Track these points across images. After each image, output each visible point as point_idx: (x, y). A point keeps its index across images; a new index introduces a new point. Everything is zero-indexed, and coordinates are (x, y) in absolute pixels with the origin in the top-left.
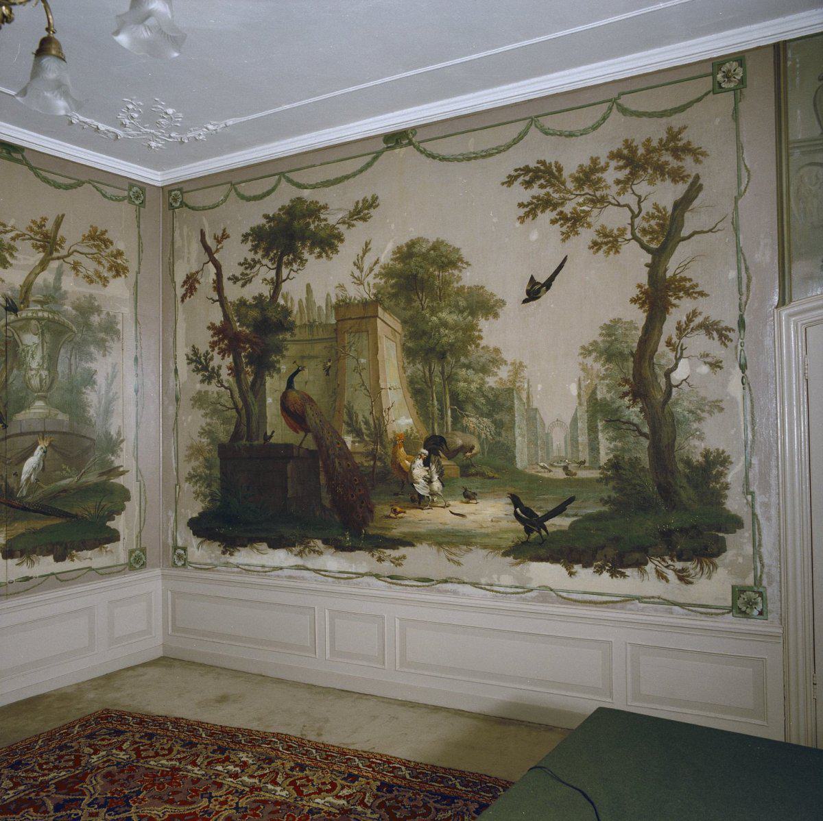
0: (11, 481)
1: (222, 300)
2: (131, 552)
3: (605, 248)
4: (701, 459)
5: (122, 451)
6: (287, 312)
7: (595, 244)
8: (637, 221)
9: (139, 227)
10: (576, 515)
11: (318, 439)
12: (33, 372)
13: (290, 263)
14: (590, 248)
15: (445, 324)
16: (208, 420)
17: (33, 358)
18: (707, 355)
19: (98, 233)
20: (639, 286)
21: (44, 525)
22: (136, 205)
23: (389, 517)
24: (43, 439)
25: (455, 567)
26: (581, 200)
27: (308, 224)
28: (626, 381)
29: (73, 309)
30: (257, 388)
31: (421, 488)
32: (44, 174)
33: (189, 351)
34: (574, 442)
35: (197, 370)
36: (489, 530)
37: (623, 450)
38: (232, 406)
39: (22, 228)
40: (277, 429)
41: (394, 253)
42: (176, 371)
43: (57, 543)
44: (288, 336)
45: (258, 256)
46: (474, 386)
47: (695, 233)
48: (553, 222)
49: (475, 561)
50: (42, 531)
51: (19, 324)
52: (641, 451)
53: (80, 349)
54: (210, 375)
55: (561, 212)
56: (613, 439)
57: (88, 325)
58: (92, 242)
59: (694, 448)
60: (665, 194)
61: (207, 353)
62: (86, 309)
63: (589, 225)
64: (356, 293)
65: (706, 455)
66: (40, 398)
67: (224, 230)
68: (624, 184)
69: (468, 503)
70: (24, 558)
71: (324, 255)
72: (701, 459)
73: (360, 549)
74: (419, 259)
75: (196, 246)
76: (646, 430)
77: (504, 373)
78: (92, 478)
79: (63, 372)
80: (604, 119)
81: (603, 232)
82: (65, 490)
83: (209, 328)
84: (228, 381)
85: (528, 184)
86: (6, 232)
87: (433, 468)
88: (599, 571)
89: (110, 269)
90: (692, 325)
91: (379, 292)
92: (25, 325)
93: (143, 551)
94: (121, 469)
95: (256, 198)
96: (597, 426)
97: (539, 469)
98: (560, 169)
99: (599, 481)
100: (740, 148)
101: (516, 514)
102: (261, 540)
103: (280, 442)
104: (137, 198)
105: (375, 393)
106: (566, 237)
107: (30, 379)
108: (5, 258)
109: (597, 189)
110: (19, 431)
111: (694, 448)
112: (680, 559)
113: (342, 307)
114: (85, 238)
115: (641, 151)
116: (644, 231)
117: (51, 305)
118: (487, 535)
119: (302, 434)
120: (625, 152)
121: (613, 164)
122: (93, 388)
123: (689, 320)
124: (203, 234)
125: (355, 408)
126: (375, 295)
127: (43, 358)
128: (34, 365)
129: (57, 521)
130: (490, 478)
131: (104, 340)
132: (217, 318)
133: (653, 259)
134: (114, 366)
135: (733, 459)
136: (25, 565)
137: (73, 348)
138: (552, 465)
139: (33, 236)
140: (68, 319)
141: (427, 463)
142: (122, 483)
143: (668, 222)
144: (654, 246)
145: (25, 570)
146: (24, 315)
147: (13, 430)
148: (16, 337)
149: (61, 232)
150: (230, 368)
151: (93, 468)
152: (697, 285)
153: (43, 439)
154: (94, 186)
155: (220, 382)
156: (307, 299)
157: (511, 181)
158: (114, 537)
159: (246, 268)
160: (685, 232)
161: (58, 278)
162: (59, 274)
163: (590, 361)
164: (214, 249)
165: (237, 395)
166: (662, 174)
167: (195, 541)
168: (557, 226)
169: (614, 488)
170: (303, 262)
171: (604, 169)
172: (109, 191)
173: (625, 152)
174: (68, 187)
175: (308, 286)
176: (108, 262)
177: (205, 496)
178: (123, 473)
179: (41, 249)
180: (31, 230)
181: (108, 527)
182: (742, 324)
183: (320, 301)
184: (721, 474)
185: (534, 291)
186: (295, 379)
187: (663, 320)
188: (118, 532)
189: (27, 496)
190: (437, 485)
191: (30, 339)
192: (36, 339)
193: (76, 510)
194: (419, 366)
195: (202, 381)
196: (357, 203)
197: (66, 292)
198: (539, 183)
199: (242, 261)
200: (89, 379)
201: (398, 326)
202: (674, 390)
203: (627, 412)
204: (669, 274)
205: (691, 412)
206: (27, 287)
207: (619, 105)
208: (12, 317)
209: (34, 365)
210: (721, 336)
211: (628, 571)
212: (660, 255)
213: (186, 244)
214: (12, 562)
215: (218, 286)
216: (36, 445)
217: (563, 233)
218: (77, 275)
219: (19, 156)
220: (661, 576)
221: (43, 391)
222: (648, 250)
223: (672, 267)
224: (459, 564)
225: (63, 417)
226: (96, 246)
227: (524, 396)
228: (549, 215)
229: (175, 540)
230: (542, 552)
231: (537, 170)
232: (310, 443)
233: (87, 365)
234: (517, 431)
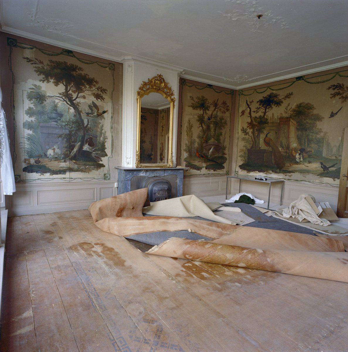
0: (208, 154)
1: (251, 117)
2: (226, 171)
6: (267, 119)
10: (337, 167)
11: (272, 148)
13: (269, 108)
15: (307, 123)
16: (245, 144)
23: (289, 166)
25: (305, 178)
27: (274, 99)
30: (258, 136)
31: (298, 160)
32: (217, 91)
33: (242, 128)
35: (243, 132)
36: (314, 170)
38: (251, 140)
40: (262, 146)
41: (296, 106)
42: (238, 133)
44: (267, 125)
45: (261, 106)
46: (314, 137)
48: (340, 98)
49: (310, 176)
54: (246, 133)
61: (246, 129)
62: (222, 119)
64: (285, 115)
67: (252, 100)
69: (309, 164)
71: (278, 106)
73: (281, 173)
74: (303, 107)
75: (245, 104)
77: (322, 134)
78: (220, 155)
83: (247, 123)
84: (251, 135)
85: (334, 89)
87: (301, 156)
91: (291, 115)
93: (229, 171)
95: (261, 93)
97: (329, 157)
98: (343, 85)
101: (321, 167)
102: (257, 170)
103: (263, 149)
105: (288, 138)
106: (343, 102)
113: (281, 119)
118: (314, 171)
119: (269, 147)
124: (247, 101)
125: (283, 142)
126: (290, 116)
129: (214, 163)
130: (315, 158)
131: (224, 126)
132: (249, 121)
138: (332, 156)
141: (300, 154)
145: (209, 172)
147: (208, 144)
150: (252, 132)
155: (249, 135)
156: (272, 117)
157: (329, 88)
158: (223, 168)
159: (257, 109)
161: (217, 113)
162: (217, 111)
164: (249, 105)
165: (253, 138)
167: (240, 170)
168: (341, 99)
170: (272, 108)
175: (273, 114)
177: (243, 160)
178: (226, 154)
180: (213, 103)
181: (223, 166)
183: (276, 117)
185: (332, 115)
186: (268, 135)
190: (302, 159)
191: (212, 126)
193: (217, 161)
194: (300, 132)
195: (245, 135)
196: (287, 94)
198: (337, 89)
199: (256, 107)
201: (295, 123)
206: (212, 115)
213: (242, 103)
215: (250, 113)
217: (342, 101)
224: (306, 177)
226: (224, 105)
227: (327, 140)
228: (339, 97)
229: (235, 169)
230: (327, 175)
231: (337, 86)
232: (270, 149)
234: (324, 148)
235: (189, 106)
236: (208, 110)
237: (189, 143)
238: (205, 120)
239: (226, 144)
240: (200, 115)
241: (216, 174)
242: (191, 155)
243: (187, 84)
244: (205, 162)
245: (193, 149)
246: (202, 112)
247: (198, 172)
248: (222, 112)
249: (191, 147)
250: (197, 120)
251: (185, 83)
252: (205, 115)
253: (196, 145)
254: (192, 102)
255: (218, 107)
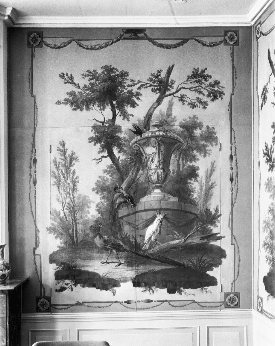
0: (138, 240)
2: (227, 295)
5: (219, 222)
9: (233, 60)
12: (153, 171)
17: (153, 162)
19: (198, 73)
21: (161, 268)
22: (231, 45)
24: (160, 214)
29: (181, 127)
32: (159, 42)
39: (145, 81)
43: (170, 281)
50: (158, 272)
51: (144, 141)
53: (187, 154)
57: (192, 137)
58: (195, 79)
62: (189, 127)
66: (157, 187)
70: (147, 288)
78: (195, 240)
79: (173, 170)
82: (175, 247)
86: (134, 85)
89: (209, 96)
92: (147, 142)
93: (237, 295)
94: (219, 235)
104: (231, 39)
107: (150, 175)
108: (134, 101)
110: (143, 209)
114: (189, 77)
117: (165, 127)
122: (196, 179)
127: (159, 161)
128: (153, 166)
131: (204, 146)
134: (213, 164)
136: (148, 292)
137: (181, 153)
139: (152, 84)
140: (177, 134)
142: (220, 246)
145: (147, 295)
146: (146, 135)
148: (141, 150)
149: (172, 77)
151: (196, 234)
153: (160, 214)
154: (196, 40)
158: (213, 282)
172: (207, 40)
174: (175, 46)
176: (208, 90)
178: (220, 238)
179: (157, 91)
180: (151, 80)
181: (208, 275)
188: (216, 279)
189: (150, 248)
191: (150, 150)
192: (154, 150)
197: (175, 117)
200: (193, 173)
206: (149, 117)
208: (139, 138)
209: (153, 166)
214: (140, 289)
216: (154, 217)
218: (183, 104)
219: (141, 35)
221: (159, 183)
225: (174, 199)
226: (199, 82)
233: (189, 164)
235: (59, 103)
236: (133, 105)
237: (63, 208)
238: (122, 135)
239: (220, 201)
240: (103, 123)
241: (182, 303)
242: (73, 243)
243: (49, 41)
244: (129, 264)
245: (80, 227)
246: (108, 113)
247: (105, 295)
248: (192, 104)
249: (75, 220)
250: (90, 138)
251: (39, 40)
252: (119, 121)
253: (92, 213)
254: (71, 88)
255: (173, 91)
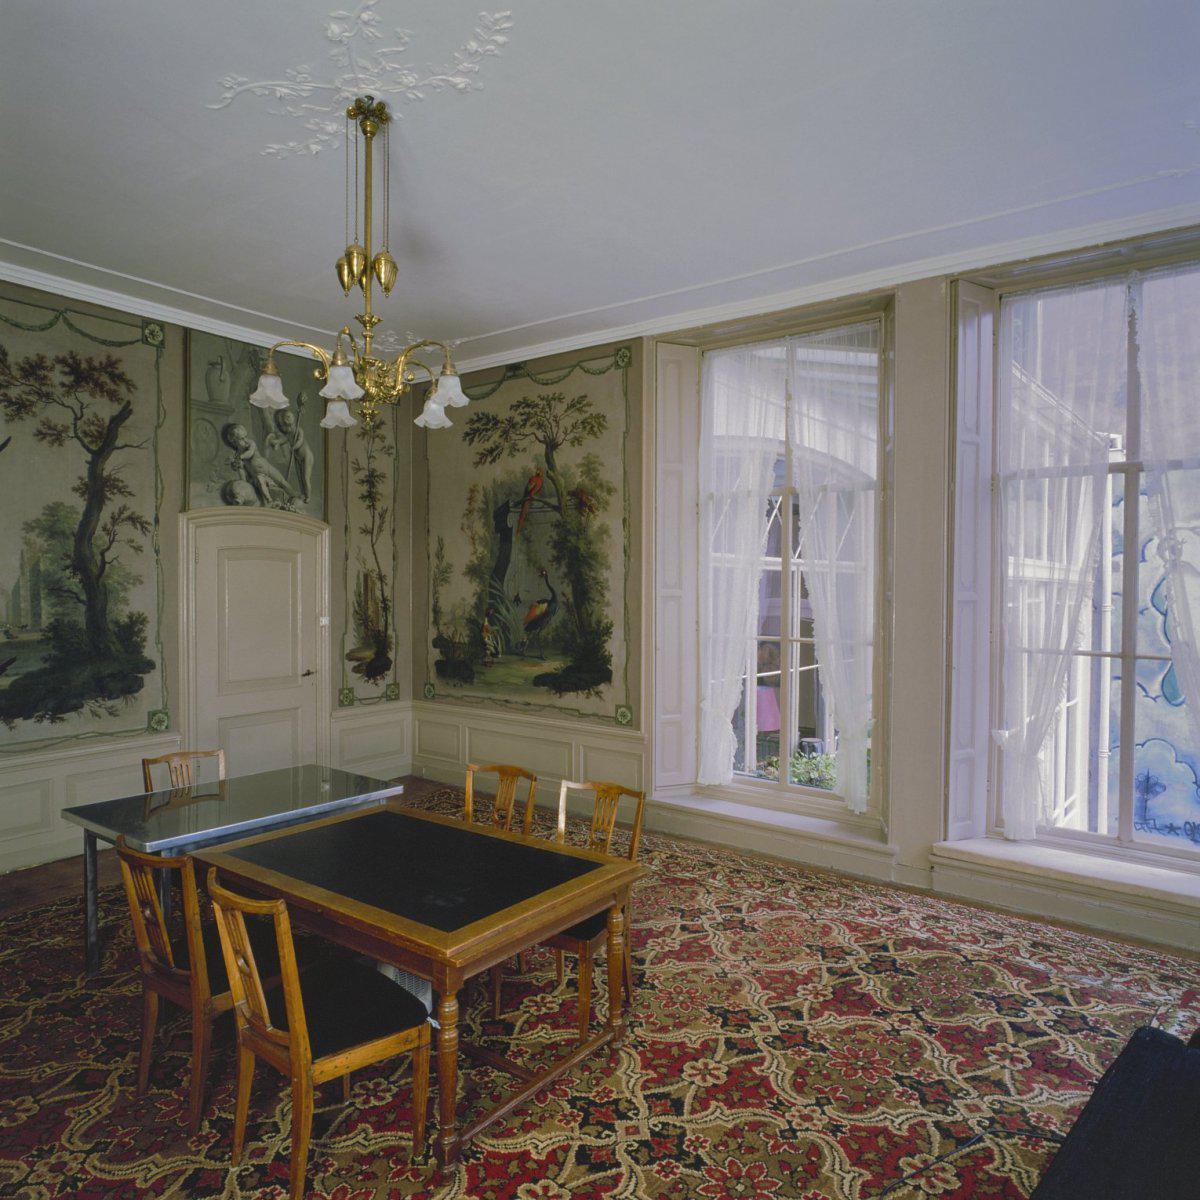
3: (48, 438)
4: (126, 620)
7: (40, 433)
8: (79, 423)
14: (35, 435)
18: (132, 541)
20: (81, 478)
26: (27, 389)
28: (68, 556)
34: (16, 609)
37: (64, 614)
47: (126, 446)
52: (79, 616)
55: (5, 395)
56: (54, 605)
59: (121, 612)
60: (105, 410)
63: (34, 415)
65: (130, 617)
68: (70, 389)
72: (126, 620)
76: (83, 597)
80: (51, 325)
81: (46, 424)
88: (40, 719)
90: (123, 516)
96: (39, 594)
99: (39, 642)
100: (159, 391)
106: (10, 419)
109: (44, 385)
111: (121, 612)
112: (110, 698)
115: (84, 365)
116: (86, 434)
120: (70, 361)
121: (58, 367)
123: (121, 512)
133: (93, 458)
135: (149, 619)
143: (105, 431)
144: (94, 447)
152: (127, 486)
160: (119, 442)
163: (32, 536)
166: (102, 391)
169: (54, 647)
171: (52, 369)
173: (70, 361)
182: (157, 521)
184: (141, 631)
187: (100, 509)
202: (107, 566)
203: (67, 583)
204: (105, 474)
205: (119, 583)
207: (65, 319)
210: (143, 527)
211: (65, 716)
212: (99, 456)
220: (95, 714)
222: (89, 450)
223: (109, 467)
